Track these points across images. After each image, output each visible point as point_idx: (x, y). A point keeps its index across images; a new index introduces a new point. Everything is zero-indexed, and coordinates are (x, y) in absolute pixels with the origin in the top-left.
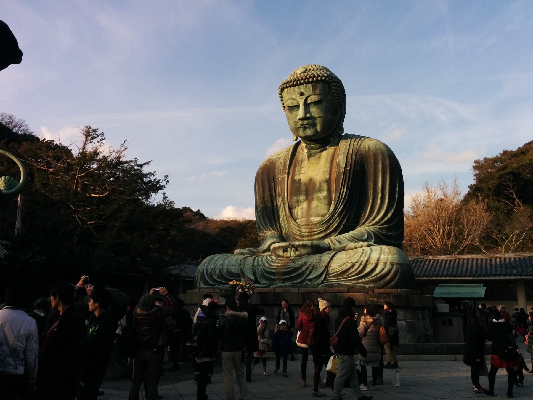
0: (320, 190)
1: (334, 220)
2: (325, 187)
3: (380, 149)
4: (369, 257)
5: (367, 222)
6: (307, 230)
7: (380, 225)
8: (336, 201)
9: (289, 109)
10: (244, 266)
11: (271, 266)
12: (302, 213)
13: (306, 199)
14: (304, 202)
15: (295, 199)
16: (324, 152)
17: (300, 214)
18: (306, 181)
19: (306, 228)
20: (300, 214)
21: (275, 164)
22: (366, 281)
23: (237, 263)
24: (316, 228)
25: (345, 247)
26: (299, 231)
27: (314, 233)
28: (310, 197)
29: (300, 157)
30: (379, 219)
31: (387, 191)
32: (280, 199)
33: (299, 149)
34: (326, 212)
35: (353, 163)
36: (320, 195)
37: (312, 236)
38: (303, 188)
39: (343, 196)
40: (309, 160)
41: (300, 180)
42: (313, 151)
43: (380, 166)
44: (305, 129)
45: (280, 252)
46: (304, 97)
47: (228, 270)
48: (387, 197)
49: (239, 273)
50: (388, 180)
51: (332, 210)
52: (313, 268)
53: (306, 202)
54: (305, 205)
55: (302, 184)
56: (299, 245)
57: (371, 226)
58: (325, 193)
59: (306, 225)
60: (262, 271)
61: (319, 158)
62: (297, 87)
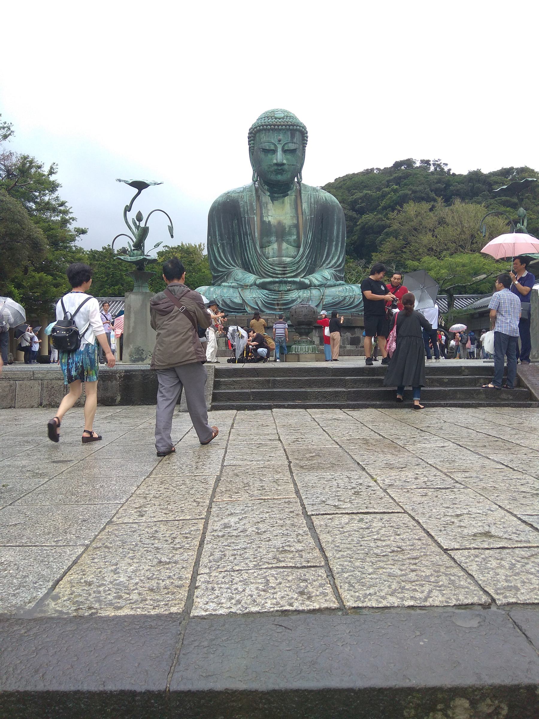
0: (290, 234)
1: (303, 262)
2: (294, 231)
3: (335, 202)
5: (324, 265)
6: (281, 269)
13: (277, 241)
15: (265, 239)
17: (271, 254)
19: (279, 267)
20: (271, 254)
21: (237, 202)
25: (325, 284)
28: (280, 240)
29: (263, 198)
34: (295, 253)
35: (316, 212)
36: (290, 238)
37: (284, 274)
41: (269, 222)
42: (276, 195)
44: (277, 174)
45: (271, 287)
46: (283, 143)
47: (231, 301)
48: (340, 245)
53: (276, 243)
54: (275, 246)
56: (290, 282)
57: (329, 268)
59: (279, 264)
60: (262, 302)
61: (283, 202)
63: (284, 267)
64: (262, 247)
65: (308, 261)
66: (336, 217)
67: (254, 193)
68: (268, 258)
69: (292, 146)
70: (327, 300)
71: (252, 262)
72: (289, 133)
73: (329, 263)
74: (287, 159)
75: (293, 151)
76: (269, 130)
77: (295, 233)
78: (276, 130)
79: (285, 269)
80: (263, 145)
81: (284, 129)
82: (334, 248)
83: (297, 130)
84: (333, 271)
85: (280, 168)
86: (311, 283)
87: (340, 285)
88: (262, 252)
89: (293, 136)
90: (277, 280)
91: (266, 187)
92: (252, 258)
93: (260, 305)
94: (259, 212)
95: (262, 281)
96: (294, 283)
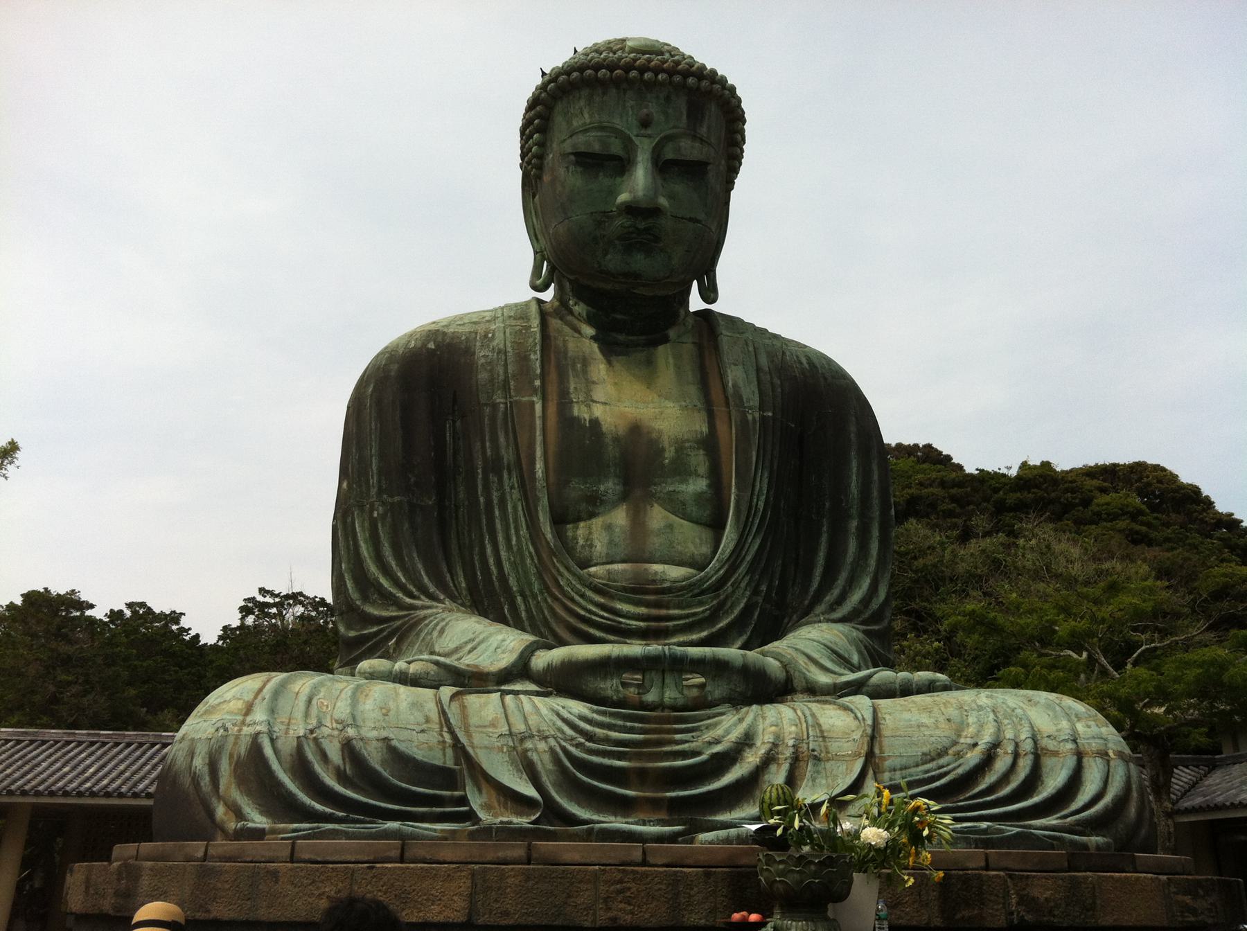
0: (681, 470)
1: (736, 585)
2: (699, 461)
4: (1032, 727)
5: (819, 609)
6: (642, 610)
7: (862, 623)
8: (743, 518)
9: (577, 163)
10: (469, 735)
11: (590, 737)
12: (611, 542)
14: (615, 505)
15: (577, 488)
16: (661, 348)
18: (621, 431)
21: (468, 352)
22: (1078, 823)
23: (428, 721)
24: (679, 607)
26: (603, 607)
27: (670, 624)
29: (571, 345)
30: (861, 601)
31: (876, 513)
32: (510, 480)
33: (555, 323)
34: (705, 549)
38: (612, 452)
39: (761, 505)
40: (609, 363)
41: (595, 423)
42: (621, 337)
43: (853, 428)
48: (875, 533)
49: (450, 763)
50: (876, 477)
51: (731, 546)
52: (796, 759)
55: (608, 440)
56: (698, 665)
58: (698, 485)
61: (650, 363)
62: (630, 94)
63: (658, 605)
64: (561, 519)
65: (758, 585)
66: (853, 428)
67: (535, 323)
68: (585, 564)
69: (689, 149)
70: (897, 762)
71: (512, 582)
72: (681, 103)
73: (840, 601)
74: (671, 197)
75: (693, 170)
76: (603, 84)
77: (702, 470)
78: (631, 82)
79: (663, 612)
80: (581, 139)
81: (662, 84)
82: (852, 546)
83: (709, 93)
84: (861, 635)
85: (642, 225)
86: (789, 680)
87: (930, 688)
88: (560, 535)
89: (695, 113)
90: (635, 649)
91: (580, 309)
92: (514, 565)
93: (546, 780)
94: (553, 390)
95: (558, 654)
96: (718, 668)
